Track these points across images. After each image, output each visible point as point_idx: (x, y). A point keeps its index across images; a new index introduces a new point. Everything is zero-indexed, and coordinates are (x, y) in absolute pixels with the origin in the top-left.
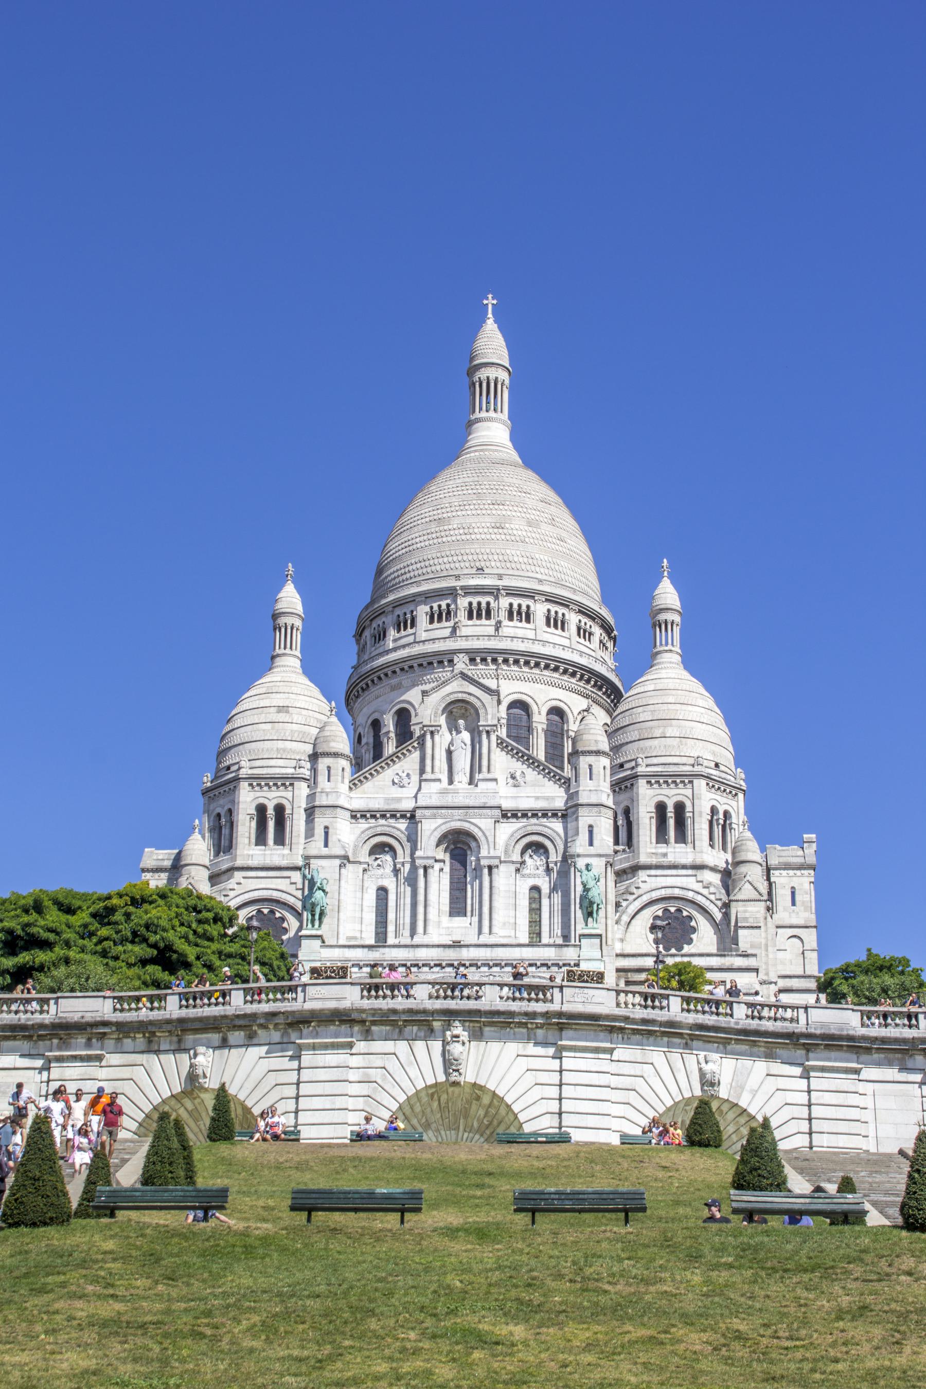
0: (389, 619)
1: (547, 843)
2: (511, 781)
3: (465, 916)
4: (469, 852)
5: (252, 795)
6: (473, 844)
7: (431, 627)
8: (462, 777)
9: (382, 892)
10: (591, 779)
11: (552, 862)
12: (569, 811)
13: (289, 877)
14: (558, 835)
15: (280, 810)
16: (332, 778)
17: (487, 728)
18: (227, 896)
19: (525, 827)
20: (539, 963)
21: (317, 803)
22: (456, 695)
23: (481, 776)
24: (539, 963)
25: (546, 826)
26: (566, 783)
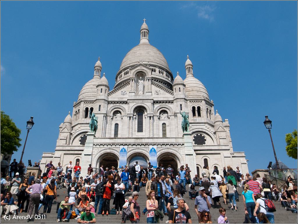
1: (167, 110)
3: (142, 131)
5: (85, 105)
8: (141, 93)
9: (117, 125)
10: (180, 91)
11: (169, 116)
12: (174, 101)
14: (171, 108)
17: (148, 78)
19: (160, 106)
20: (170, 144)
21: (97, 99)
23: (147, 91)
24: (170, 144)
25: (167, 105)
26: (172, 94)
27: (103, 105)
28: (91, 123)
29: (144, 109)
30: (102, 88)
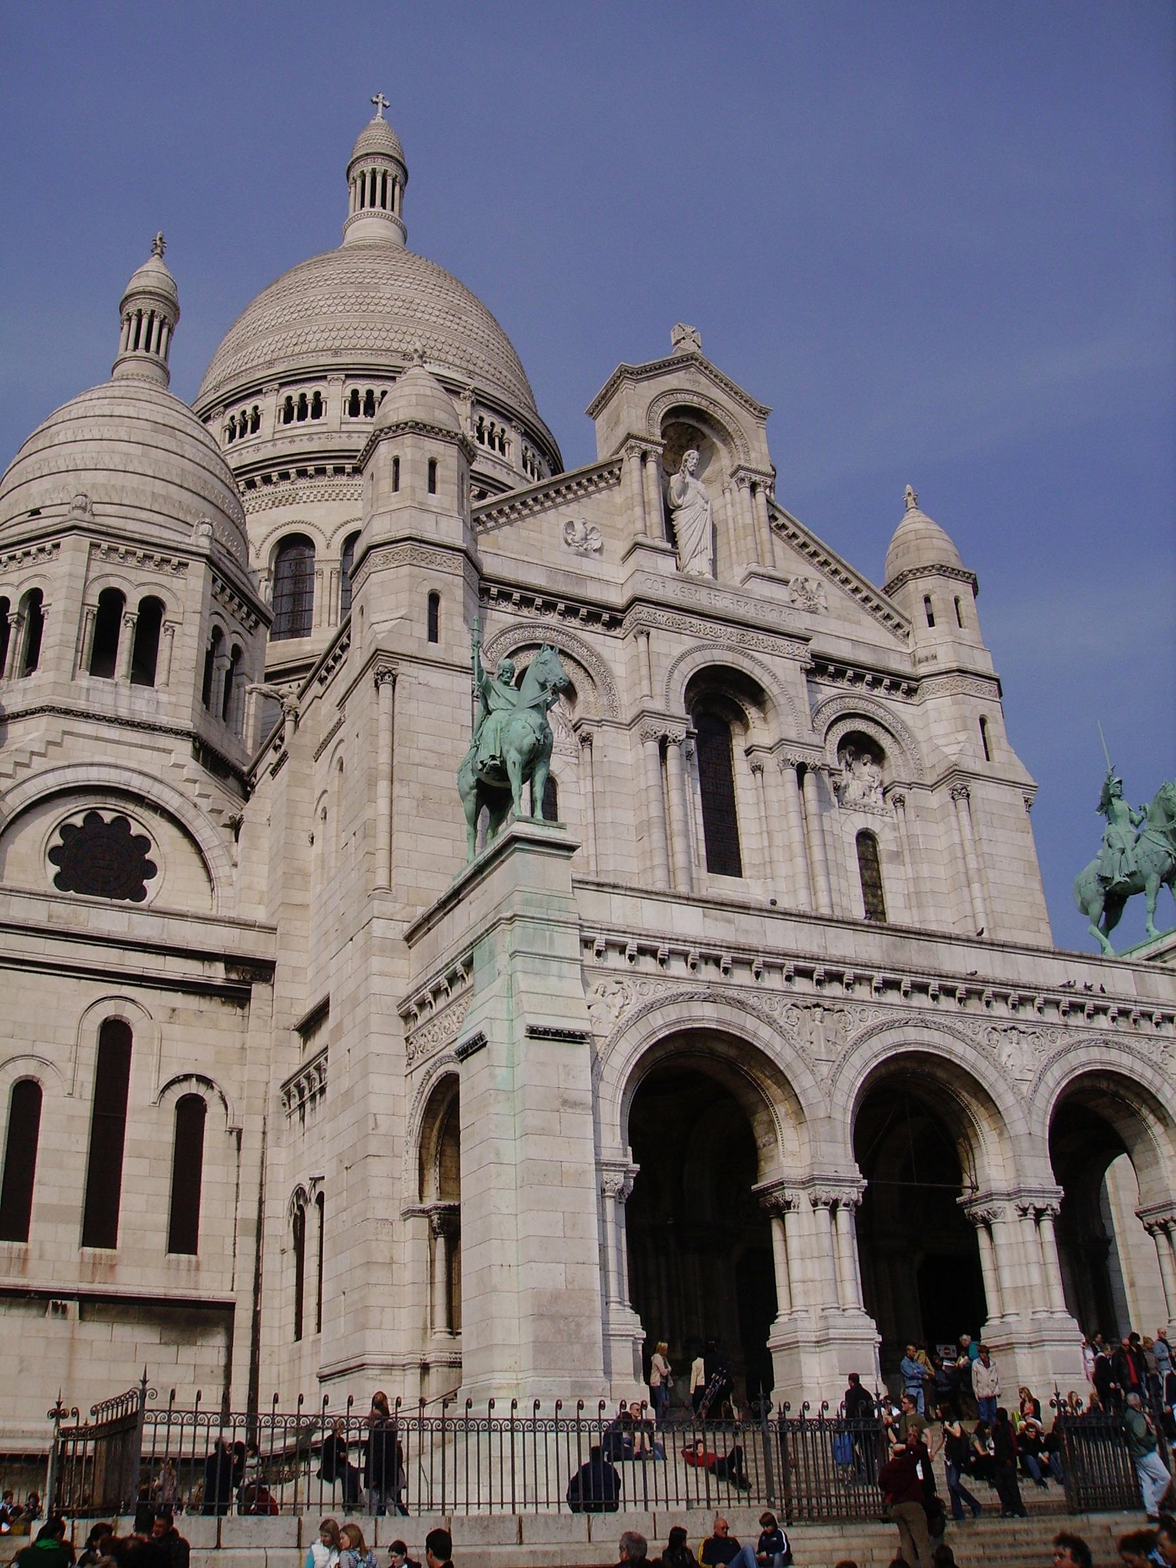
0: (270, 404)
1: (885, 741)
2: (796, 596)
4: (736, 729)
5: (97, 568)
6: (752, 713)
7: (354, 419)
10: (960, 626)
12: (925, 683)
13: (170, 752)
14: (906, 728)
15: (152, 609)
16: (438, 486)
17: (756, 478)
18: (28, 766)
21: (414, 533)
22: (688, 397)
27: (459, 594)
28: (529, 740)
29: (742, 697)
30: (439, 458)
